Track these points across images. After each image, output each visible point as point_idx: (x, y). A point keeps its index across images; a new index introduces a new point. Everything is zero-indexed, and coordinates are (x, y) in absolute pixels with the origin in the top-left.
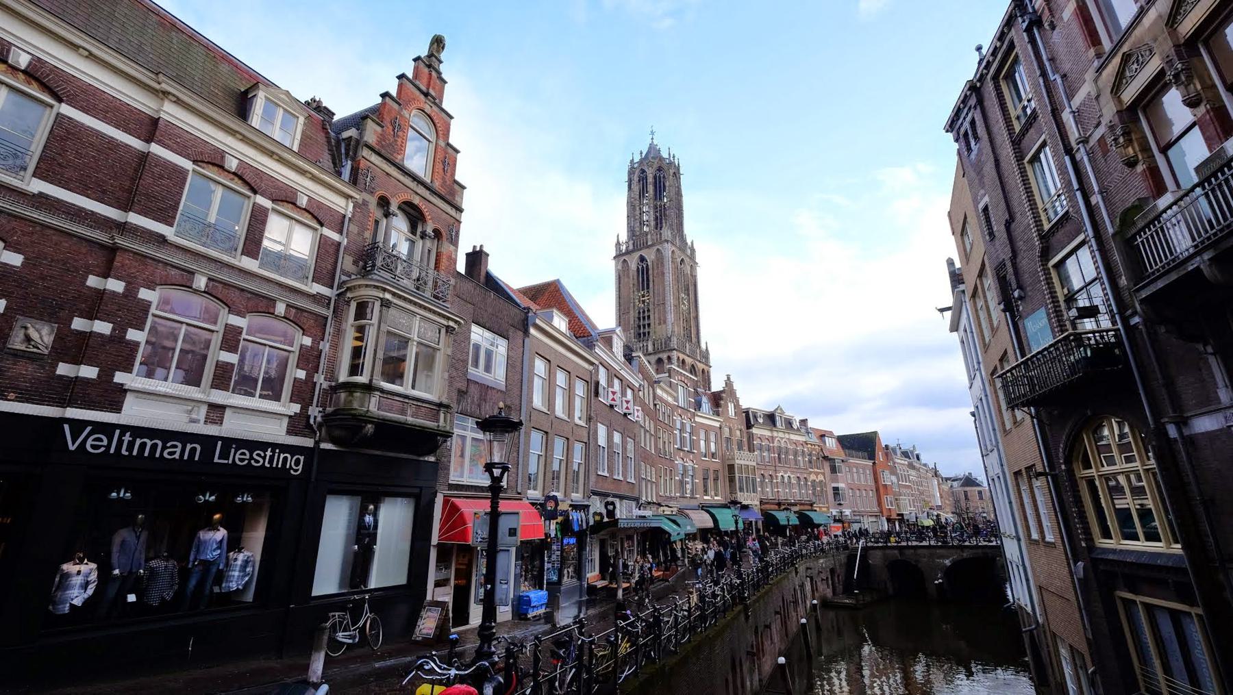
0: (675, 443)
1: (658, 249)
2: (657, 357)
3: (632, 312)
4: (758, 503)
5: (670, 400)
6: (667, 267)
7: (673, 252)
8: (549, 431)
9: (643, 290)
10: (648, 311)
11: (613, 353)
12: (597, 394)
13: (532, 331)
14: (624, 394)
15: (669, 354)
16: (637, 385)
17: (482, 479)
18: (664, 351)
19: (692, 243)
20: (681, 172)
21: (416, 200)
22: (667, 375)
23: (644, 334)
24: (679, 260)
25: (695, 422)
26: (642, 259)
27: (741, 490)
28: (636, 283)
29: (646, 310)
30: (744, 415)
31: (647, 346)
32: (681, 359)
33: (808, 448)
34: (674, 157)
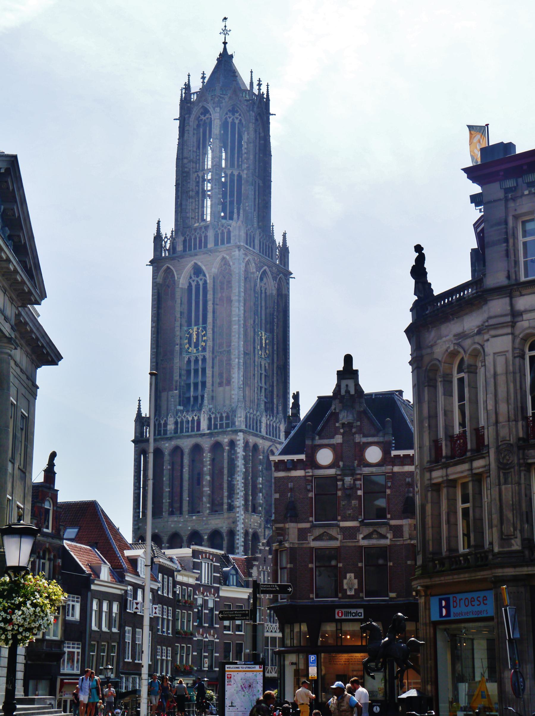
1: (224, 258)
3: (177, 360)
5: (192, 581)
6: (235, 290)
7: (248, 263)
9: (197, 324)
10: (204, 360)
11: (137, 574)
12: (126, 608)
13: (93, 587)
15: (233, 437)
16: (156, 588)
18: (224, 433)
19: (284, 235)
20: (271, 111)
21: (47, 546)
23: (196, 398)
24: (259, 274)
25: (219, 597)
26: (198, 271)
28: (186, 312)
29: (200, 358)
32: (251, 445)
34: (259, 85)
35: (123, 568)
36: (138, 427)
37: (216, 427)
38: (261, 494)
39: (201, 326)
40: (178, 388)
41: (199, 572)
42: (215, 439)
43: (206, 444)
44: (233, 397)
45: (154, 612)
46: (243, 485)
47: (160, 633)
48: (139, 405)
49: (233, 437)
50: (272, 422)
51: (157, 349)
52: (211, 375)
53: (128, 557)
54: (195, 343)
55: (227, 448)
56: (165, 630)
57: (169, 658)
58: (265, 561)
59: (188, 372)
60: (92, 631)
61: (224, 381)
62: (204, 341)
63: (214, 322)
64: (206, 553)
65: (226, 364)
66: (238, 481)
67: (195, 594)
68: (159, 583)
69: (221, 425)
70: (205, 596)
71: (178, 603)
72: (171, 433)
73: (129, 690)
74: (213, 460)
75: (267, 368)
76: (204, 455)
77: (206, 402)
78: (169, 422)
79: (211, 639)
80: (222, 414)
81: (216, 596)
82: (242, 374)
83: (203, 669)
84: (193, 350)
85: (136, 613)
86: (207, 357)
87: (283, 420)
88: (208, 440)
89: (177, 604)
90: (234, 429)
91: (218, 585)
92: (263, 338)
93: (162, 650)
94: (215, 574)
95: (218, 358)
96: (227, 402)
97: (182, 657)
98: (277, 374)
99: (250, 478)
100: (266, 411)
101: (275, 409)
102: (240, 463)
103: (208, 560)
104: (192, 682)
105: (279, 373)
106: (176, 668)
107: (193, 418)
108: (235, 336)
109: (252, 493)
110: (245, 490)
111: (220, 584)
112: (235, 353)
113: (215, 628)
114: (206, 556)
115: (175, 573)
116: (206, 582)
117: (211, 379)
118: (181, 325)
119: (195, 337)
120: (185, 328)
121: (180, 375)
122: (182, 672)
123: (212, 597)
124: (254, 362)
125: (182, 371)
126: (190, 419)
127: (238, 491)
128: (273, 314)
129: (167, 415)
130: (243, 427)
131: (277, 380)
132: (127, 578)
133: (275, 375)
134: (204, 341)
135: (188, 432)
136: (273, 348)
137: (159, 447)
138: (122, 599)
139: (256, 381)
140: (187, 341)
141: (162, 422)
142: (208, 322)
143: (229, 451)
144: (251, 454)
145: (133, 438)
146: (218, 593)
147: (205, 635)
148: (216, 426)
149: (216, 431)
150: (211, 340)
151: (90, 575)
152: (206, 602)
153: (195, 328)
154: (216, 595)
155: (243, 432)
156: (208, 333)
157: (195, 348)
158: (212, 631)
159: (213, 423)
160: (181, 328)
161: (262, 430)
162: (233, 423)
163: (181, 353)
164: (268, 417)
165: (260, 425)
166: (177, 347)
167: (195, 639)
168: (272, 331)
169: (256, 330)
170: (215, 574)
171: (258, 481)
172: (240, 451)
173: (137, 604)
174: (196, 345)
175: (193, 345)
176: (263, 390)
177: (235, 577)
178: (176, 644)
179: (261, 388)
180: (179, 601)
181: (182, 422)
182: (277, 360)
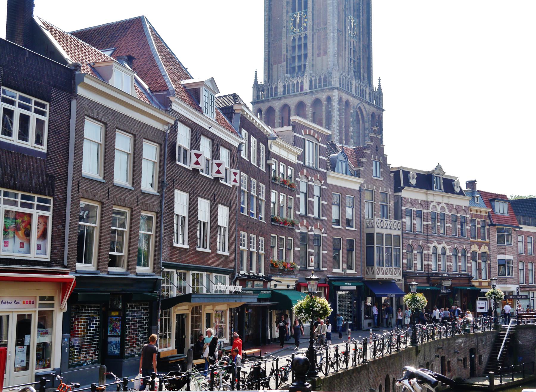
0: (297, 208)
2: (314, 97)
3: (284, 39)
4: (401, 277)
5: (293, 159)
8: (105, 200)
9: (300, 9)
10: (306, 37)
11: (200, 110)
13: (81, 91)
14: (215, 154)
15: (330, 94)
17: (19, 252)
18: (322, 91)
22: (291, 128)
23: (299, 67)
25: (326, 184)
27: (381, 263)
29: (302, 36)
30: (392, 175)
31: (302, 82)
32: (344, 100)
33: (472, 215)
35: (168, 90)
36: (255, 92)
37: (316, 87)
38: (352, 140)
39: (303, 10)
40: (285, 60)
41: (302, 150)
42: (316, 96)
43: (308, 100)
44: (329, 63)
45: (232, 179)
46: (338, 131)
47: (245, 214)
48: (256, 75)
49: (330, 94)
50: (360, 86)
51: (269, 32)
52: (311, 48)
53: (185, 86)
54: (298, 24)
55: (325, 103)
56: (254, 212)
57: (262, 252)
58: (377, 150)
59: (294, 47)
60: (80, 179)
61: (322, 53)
62: (306, 22)
63: (313, 7)
64: (310, 129)
65: (323, 39)
66: (334, 128)
67: (296, 176)
68: (242, 138)
69: (320, 87)
70: (309, 181)
71: (273, 181)
72: (280, 94)
73: (187, 293)
74: (314, 113)
75: (355, 45)
76: (307, 109)
77: (307, 68)
78: (278, 86)
79: (317, 232)
80: (320, 77)
81: (323, 182)
82: (336, 45)
83: (308, 268)
84: (297, 30)
85: (196, 171)
86: (308, 34)
87: (368, 85)
88: (310, 97)
89: (272, 182)
90: (330, 87)
91: (325, 171)
92: (352, 21)
93: (249, 238)
94: (321, 157)
95: (316, 34)
96: (325, 68)
97: (280, 251)
98: (363, 50)
99: (343, 126)
100: (356, 77)
101: (362, 77)
102: (335, 114)
103: (313, 138)
104: (294, 283)
105: (364, 51)
106: (272, 265)
107: (298, 81)
108: (330, 15)
109: (345, 138)
110: (339, 135)
111: (327, 169)
112: (330, 29)
113: (322, 220)
114: (310, 132)
115: (269, 142)
116: (311, 165)
117: (311, 51)
118: (287, 12)
119: (298, 20)
120: (291, 14)
121: (287, 51)
122: (281, 271)
123: (318, 183)
124: (345, 38)
125: (289, 47)
126: (295, 82)
127: (334, 136)
128: (359, 3)
129: (278, 81)
130: (338, 85)
131: (363, 55)
132: (175, 107)
133: (361, 51)
134: (306, 22)
135: (294, 92)
136: (360, 30)
137: (271, 106)
138: (165, 140)
139: (347, 53)
140: (292, 24)
141: (274, 87)
142: (308, 6)
143: (327, 105)
144: (344, 108)
145: (251, 100)
146: (325, 180)
147: (310, 228)
148: (316, 87)
149: (316, 90)
150: (311, 20)
151: (77, 67)
152: (310, 188)
153: (299, 13)
154: (323, 182)
155: (338, 89)
156: (308, 15)
157: (298, 28)
158: (318, 224)
159: (313, 84)
160: (287, 14)
161: (352, 90)
162: (330, 84)
163: (287, 34)
164: (357, 81)
165: (351, 87)
166: (285, 29)
167: (297, 231)
168: (358, 17)
169: (347, 13)
170: (321, 157)
171: (350, 130)
172: (335, 104)
173: (198, 156)
174: (300, 26)
175: (297, 27)
176: (352, 62)
177: (344, 164)
178: (272, 235)
179: (351, 59)
180: (275, 179)
181: (289, 85)
182: (363, 40)
